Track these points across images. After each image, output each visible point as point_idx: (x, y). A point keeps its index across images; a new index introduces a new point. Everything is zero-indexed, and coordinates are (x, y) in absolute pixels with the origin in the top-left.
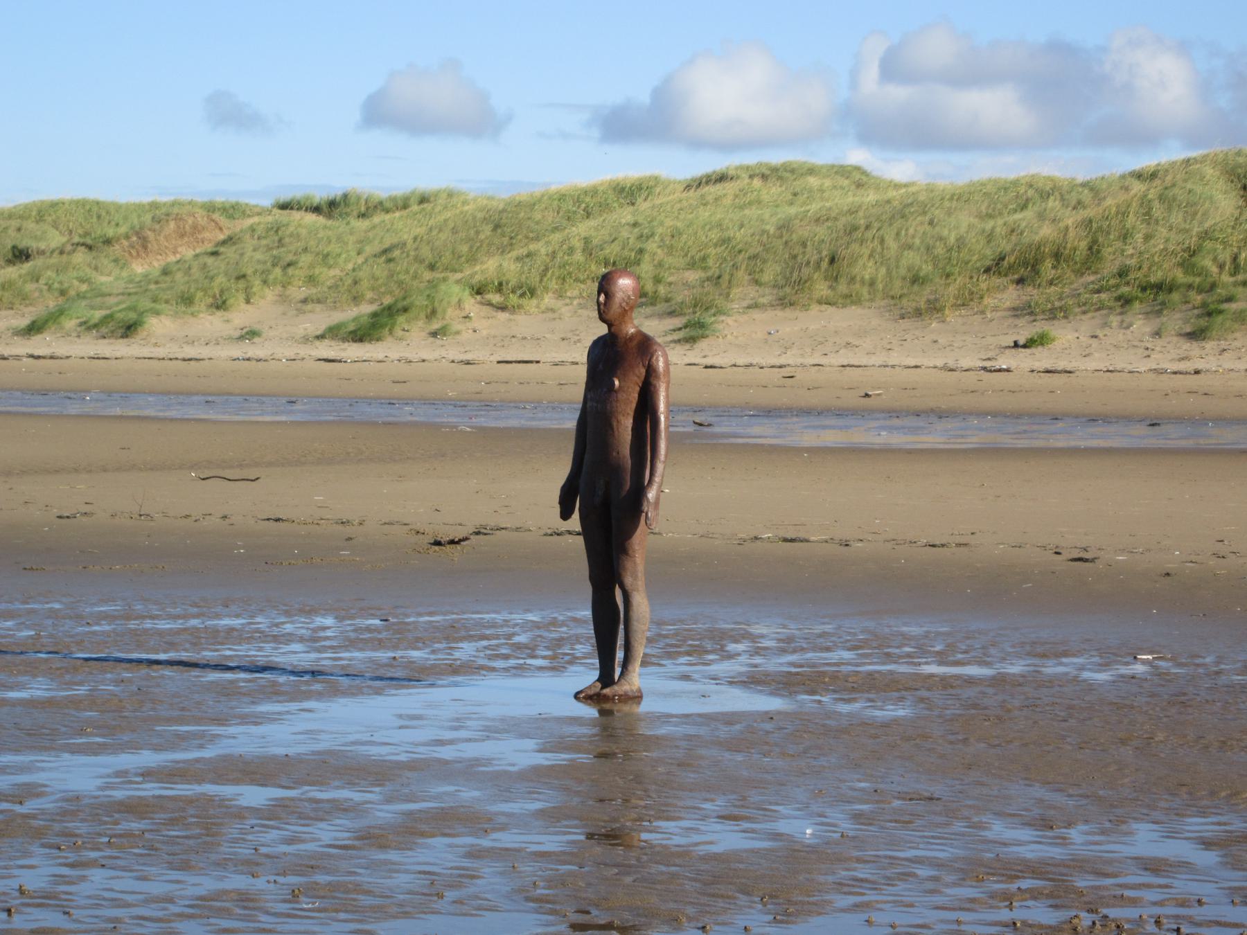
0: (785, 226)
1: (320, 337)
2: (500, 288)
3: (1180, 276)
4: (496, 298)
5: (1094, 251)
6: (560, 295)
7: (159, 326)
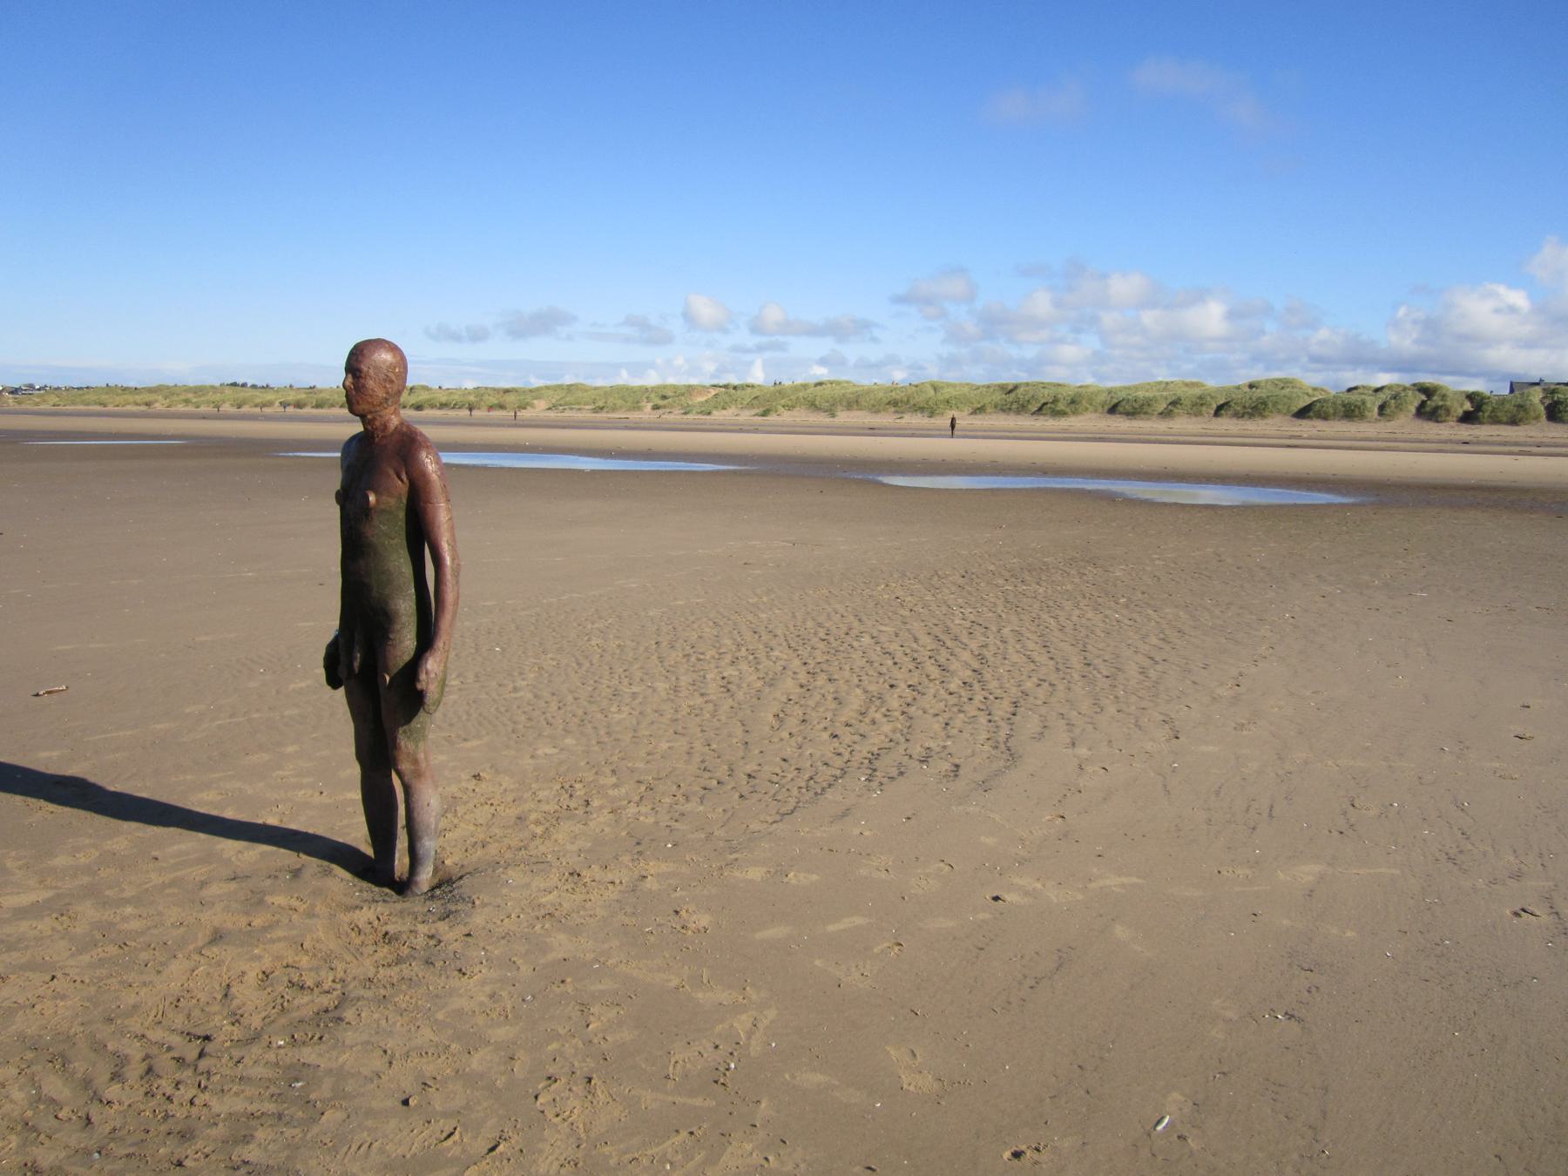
0: (844, 395)
1: (754, 415)
2: (787, 406)
3: (925, 406)
5: (908, 401)
7: (715, 412)
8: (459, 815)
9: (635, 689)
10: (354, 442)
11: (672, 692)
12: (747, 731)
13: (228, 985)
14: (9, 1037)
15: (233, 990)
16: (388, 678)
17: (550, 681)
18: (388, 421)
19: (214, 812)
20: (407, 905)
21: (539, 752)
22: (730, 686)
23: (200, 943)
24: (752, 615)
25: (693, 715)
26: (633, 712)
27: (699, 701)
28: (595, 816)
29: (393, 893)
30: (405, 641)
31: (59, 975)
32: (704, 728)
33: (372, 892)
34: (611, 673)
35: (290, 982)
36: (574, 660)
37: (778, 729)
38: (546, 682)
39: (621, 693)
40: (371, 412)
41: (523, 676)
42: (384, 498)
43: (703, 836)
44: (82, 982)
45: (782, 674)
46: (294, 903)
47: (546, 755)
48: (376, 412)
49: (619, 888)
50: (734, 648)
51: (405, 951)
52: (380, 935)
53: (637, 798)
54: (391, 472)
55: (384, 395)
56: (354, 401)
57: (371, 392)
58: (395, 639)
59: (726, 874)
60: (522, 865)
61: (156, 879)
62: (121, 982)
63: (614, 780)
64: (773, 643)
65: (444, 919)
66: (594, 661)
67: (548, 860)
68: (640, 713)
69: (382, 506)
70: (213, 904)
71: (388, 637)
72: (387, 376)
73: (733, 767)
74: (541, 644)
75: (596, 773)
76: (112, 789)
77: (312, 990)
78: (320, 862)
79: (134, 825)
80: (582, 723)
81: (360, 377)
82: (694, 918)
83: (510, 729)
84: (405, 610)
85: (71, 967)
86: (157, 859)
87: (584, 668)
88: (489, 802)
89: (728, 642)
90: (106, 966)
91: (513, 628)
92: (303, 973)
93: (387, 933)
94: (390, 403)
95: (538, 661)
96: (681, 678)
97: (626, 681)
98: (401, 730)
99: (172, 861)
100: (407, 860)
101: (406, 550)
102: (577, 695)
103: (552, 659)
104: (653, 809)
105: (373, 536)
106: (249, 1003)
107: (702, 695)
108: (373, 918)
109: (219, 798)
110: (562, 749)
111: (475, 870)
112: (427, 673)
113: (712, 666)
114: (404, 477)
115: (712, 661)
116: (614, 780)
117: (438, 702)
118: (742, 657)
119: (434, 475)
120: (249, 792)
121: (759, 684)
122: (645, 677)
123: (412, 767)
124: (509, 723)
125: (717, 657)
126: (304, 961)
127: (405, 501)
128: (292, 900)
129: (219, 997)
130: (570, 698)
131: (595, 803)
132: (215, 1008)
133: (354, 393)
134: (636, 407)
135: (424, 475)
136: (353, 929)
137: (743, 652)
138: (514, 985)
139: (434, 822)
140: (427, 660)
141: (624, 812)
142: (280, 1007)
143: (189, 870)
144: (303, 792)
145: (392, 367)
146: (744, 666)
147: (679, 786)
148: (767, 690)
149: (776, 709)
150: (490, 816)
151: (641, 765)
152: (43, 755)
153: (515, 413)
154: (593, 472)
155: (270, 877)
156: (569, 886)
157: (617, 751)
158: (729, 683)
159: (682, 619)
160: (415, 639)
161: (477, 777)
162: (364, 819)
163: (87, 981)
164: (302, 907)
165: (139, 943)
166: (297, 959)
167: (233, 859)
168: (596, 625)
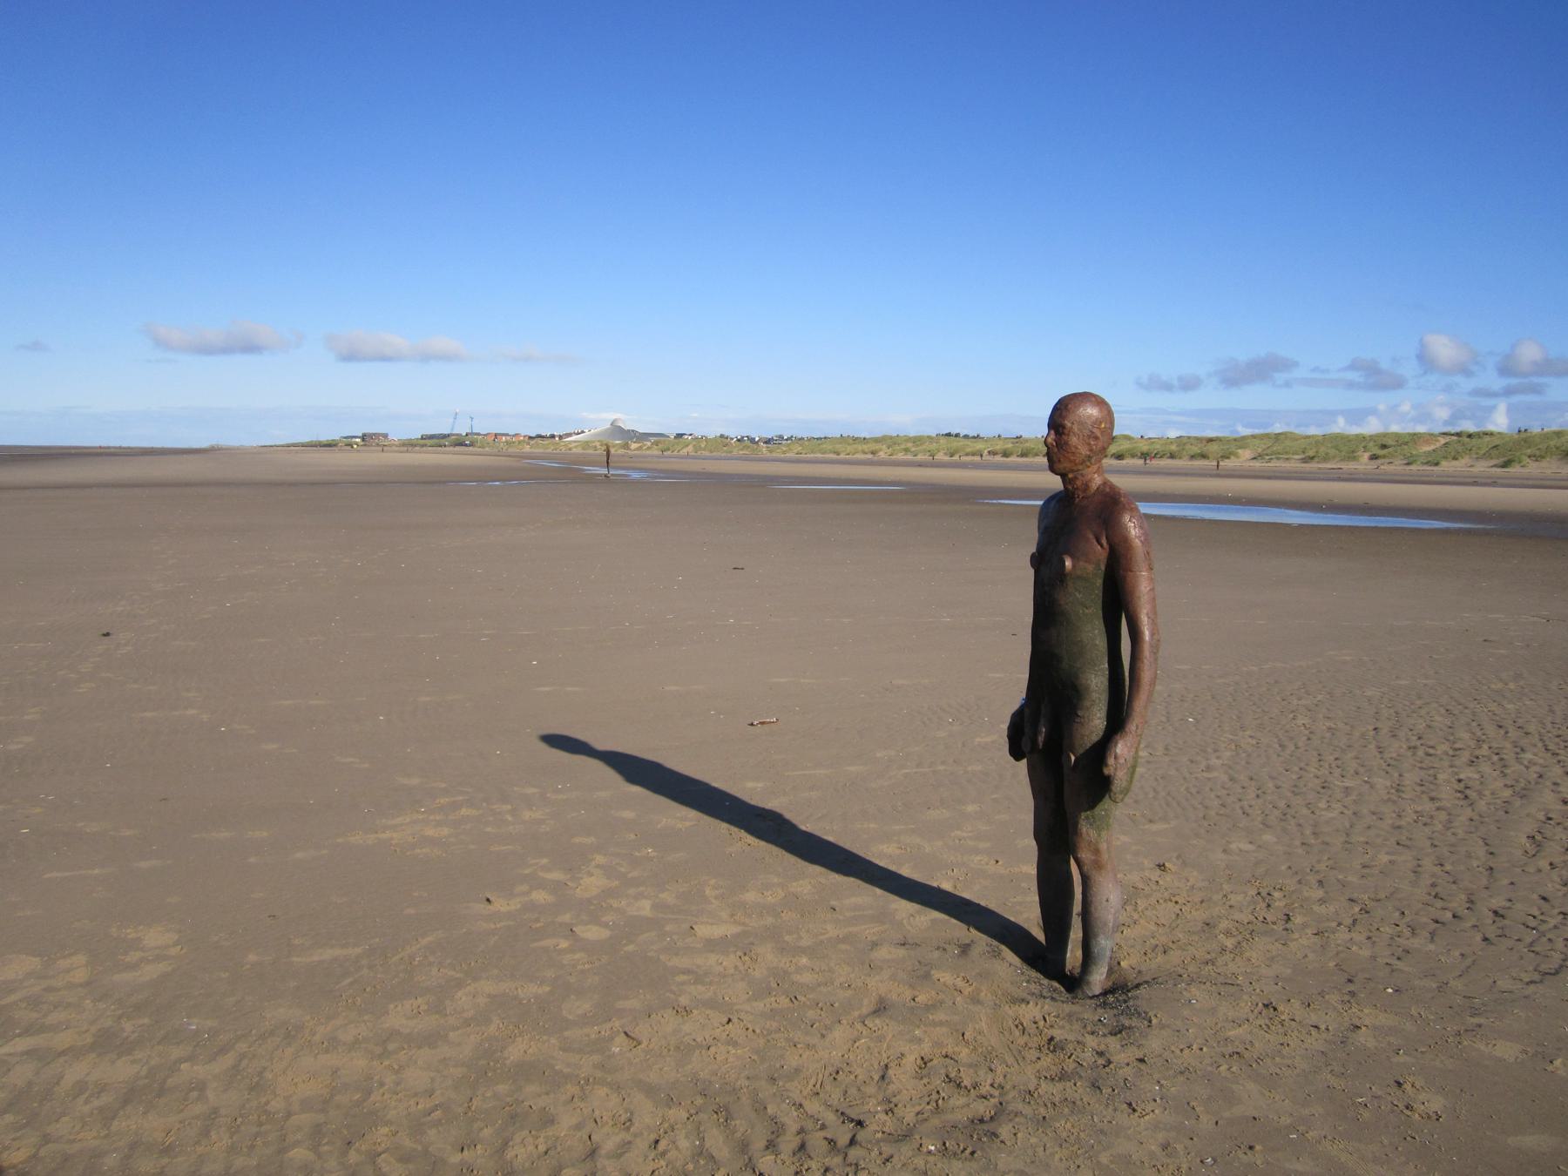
1: (1492, 467)
2: (1535, 456)
4: (1534, 459)
6: (1551, 458)
7: (1444, 463)
8: (1140, 909)
9: (1348, 783)
10: (1053, 503)
11: (1393, 791)
12: (1491, 853)
13: (886, 1066)
14: (684, 1076)
15: (890, 1072)
16: (1073, 758)
17: (1248, 763)
18: (1090, 481)
19: (893, 868)
20: (1076, 1008)
21: (1233, 846)
22: (1468, 792)
23: (865, 1011)
24: (1495, 704)
25: (1420, 824)
26: (1346, 811)
27: (1428, 806)
28: (1296, 936)
29: (1062, 989)
30: (1095, 720)
31: (735, 1020)
32: (1436, 843)
33: (1041, 985)
34: (1320, 761)
35: (947, 1076)
36: (1276, 740)
37: (1534, 855)
38: (1243, 763)
39: (1332, 785)
40: (1072, 471)
41: (1217, 754)
42: (1081, 563)
43: (1434, 986)
44: (754, 1031)
45: (1537, 783)
46: (960, 983)
47: (1241, 851)
48: (1078, 470)
49: (1324, 1035)
50: (1473, 744)
51: (1070, 1065)
52: (1045, 1039)
53: (1349, 921)
54: (1091, 536)
56: (1055, 458)
57: (1073, 449)
58: (1084, 718)
59: (1465, 1043)
60: (1208, 984)
61: (832, 931)
62: (788, 1040)
63: (1320, 893)
64: (1524, 742)
65: (1115, 1034)
66: (1300, 744)
67: (1239, 982)
68: (1355, 813)
69: (1079, 573)
70: (882, 969)
73: (1473, 898)
74: (1239, 717)
75: (1300, 882)
76: (803, 828)
77: (969, 1091)
78: (990, 940)
79: (817, 869)
80: (1284, 818)
81: (1063, 433)
82: (1422, 1096)
83: (1201, 815)
85: (747, 1012)
86: (834, 910)
87: (1288, 752)
88: (1174, 899)
89: (1466, 736)
90: (777, 1018)
91: (1209, 698)
92: (961, 1070)
93: (1052, 1039)
94: (1093, 461)
95: (1236, 738)
96: (1405, 774)
97: (1337, 772)
98: (1083, 815)
99: (848, 914)
100: (1079, 953)
101: (1102, 621)
102: (1280, 783)
103: (1251, 737)
104: (1369, 938)
105: (1067, 604)
106: (905, 1092)
107: (1432, 799)
108: (1039, 1017)
109: (898, 852)
110: (1260, 846)
111: (1154, 979)
113: (1446, 764)
114: (1104, 542)
115: (1445, 757)
116: (1320, 893)
117: (1126, 791)
118: (1483, 756)
119: (1137, 540)
120: (927, 851)
121: (1507, 793)
122: (1361, 770)
123: (1093, 858)
124: (1200, 806)
125: (1451, 752)
126: (964, 1054)
127: (1103, 568)
128: (959, 979)
129: (876, 1078)
130: (1270, 785)
131: (1298, 920)
132: (871, 1090)
133: (1056, 450)
134: (1351, 456)
135: (1126, 540)
136: (1017, 1026)
137: (1485, 750)
138: (1192, 1139)
139: (1112, 920)
141: (1332, 936)
142: (935, 1105)
143: (863, 927)
144: (979, 858)
145: (1098, 422)
146: (1486, 768)
147: (1403, 913)
148: (1518, 802)
149: (1530, 827)
150: (1174, 917)
151: (1353, 879)
152: (750, 785)
153: (1218, 462)
154: (1301, 526)
155: (938, 948)
156: (1261, 1021)
157: (1326, 858)
158: (1467, 788)
159: (1407, 703)
161: (1161, 867)
162: (1037, 898)
163: (758, 1031)
164: (968, 990)
165: (809, 999)
166: (956, 1049)
167: (905, 921)
168: (1303, 702)
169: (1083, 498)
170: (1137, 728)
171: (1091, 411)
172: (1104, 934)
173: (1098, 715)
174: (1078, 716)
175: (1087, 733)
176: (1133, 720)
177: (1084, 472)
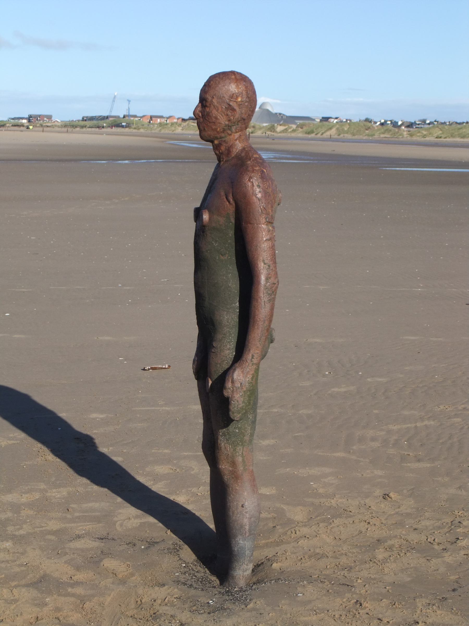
16: (210, 382)
40: (217, 138)
42: (215, 217)
54: (223, 193)
55: (227, 123)
57: (214, 120)
69: (214, 225)
71: (212, 345)
72: (230, 105)
76: (103, 449)
84: (228, 322)
94: (233, 129)
99: (77, 514)
112: (233, 382)
127: (233, 221)
139: (248, 523)
140: (235, 370)
160: (234, 350)
169: (225, 161)
170: (252, 358)
171: (233, 88)
172: (241, 535)
173: (228, 346)
174: (214, 347)
175: (219, 362)
176: (249, 350)
177: (226, 139)
